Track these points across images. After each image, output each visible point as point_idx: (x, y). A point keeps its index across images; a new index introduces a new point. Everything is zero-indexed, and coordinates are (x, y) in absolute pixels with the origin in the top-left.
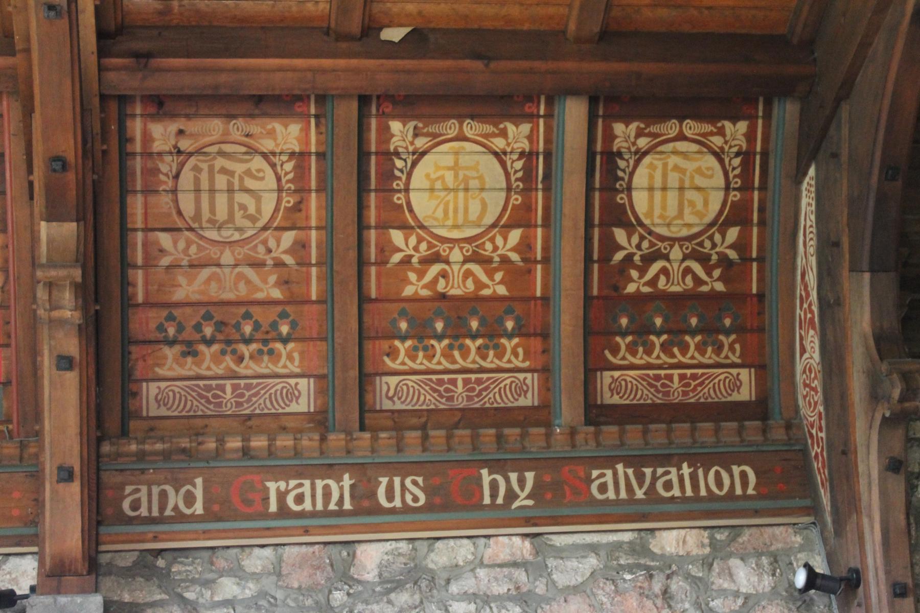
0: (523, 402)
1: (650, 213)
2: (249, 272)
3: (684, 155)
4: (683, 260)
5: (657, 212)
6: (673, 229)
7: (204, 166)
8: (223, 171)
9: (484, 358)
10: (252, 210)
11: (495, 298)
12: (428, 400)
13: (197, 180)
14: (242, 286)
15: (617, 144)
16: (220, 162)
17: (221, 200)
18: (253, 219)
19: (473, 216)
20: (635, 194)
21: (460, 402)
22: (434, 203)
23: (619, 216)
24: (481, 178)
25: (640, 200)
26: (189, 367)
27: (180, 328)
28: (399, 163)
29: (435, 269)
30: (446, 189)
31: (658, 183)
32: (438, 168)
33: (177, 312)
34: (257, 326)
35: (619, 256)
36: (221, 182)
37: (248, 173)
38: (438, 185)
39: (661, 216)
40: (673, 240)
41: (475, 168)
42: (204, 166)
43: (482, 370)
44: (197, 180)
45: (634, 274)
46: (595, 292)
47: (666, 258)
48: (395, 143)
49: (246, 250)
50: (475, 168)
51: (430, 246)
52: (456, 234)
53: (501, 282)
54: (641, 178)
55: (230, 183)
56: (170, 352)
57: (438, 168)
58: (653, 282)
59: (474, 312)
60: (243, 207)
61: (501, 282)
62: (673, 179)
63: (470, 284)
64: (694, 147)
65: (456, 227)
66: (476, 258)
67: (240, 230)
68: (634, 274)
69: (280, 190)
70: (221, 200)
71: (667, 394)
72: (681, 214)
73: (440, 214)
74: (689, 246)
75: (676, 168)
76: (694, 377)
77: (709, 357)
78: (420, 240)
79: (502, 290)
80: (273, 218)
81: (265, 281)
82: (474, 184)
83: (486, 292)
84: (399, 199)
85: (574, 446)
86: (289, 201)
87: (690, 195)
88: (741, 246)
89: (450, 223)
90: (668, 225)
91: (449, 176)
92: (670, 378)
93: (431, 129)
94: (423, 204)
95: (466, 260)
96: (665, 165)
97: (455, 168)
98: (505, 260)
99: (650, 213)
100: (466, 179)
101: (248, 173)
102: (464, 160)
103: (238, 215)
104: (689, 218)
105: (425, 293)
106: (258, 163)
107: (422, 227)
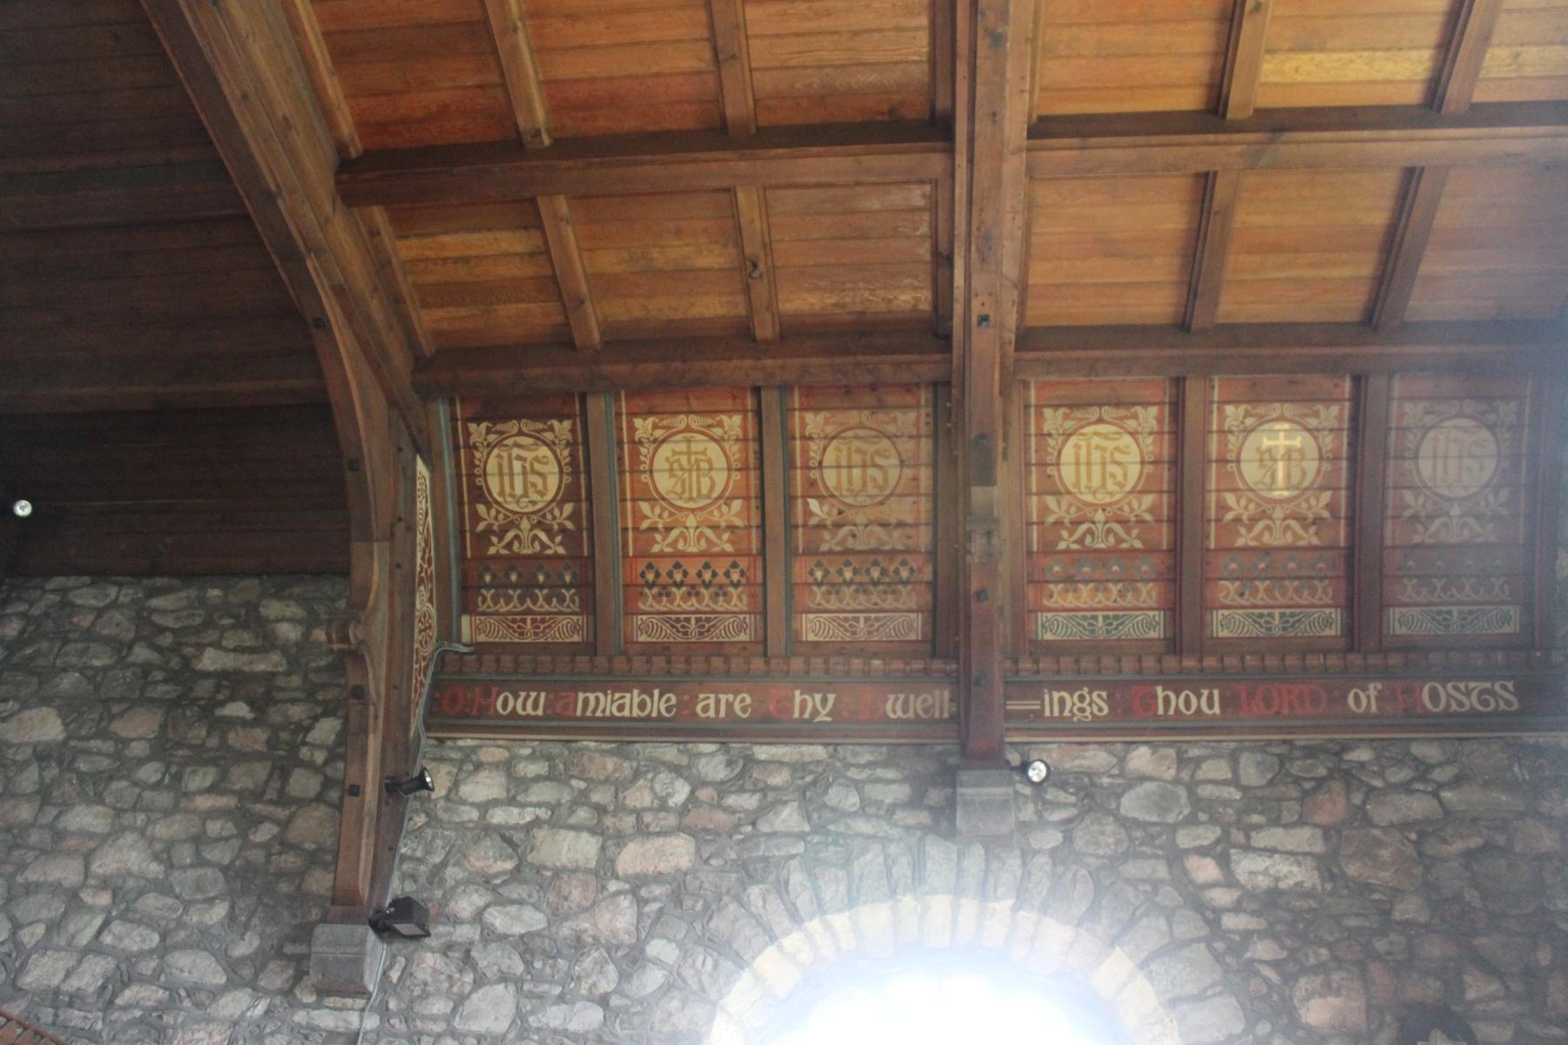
0: (912, 637)
1: (1077, 484)
2: (710, 533)
3: (1105, 437)
4: (1285, 519)
5: (1084, 482)
6: (1099, 496)
7: (505, 454)
8: (519, 458)
9: (716, 602)
10: (540, 486)
11: (556, 557)
12: (838, 635)
13: (500, 466)
14: (703, 542)
15: (1047, 427)
16: (516, 452)
17: (518, 481)
18: (542, 494)
19: (705, 491)
20: (489, 478)
21: (862, 636)
22: (673, 480)
23: (479, 494)
24: (709, 461)
25: (1068, 473)
26: (664, 605)
27: (658, 575)
28: (1051, 442)
29: (1083, 528)
30: (682, 469)
31: (844, 462)
32: (674, 453)
33: (682, 561)
34: (884, 572)
35: (481, 527)
36: (517, 466)
37: (536, 459)
38: (676, 466)
39: (1088, 487)
40: (1095, 507)
41: (704, 453)
42: (505, 454)
43: (714, 612)
44: (500, 466)
45: (494, 539)
46: (469, 554)
47: (518, 527)
48: (1047, 427)
49: (704, 514)
50: (704, 453)
51: (1079, 509)
52: (692, 505)
53: (561, 544)
54: (1068, 454)
55: (524, 467)
56: (489, 594)
57: (674, 453)
58: (1259, 537)
59: (540, 568)
60: (534, 485)
61: (561, 544)
62: (1096, 456)
63: (1111, 539)
64: (1114, 429)
65: (691, 499)
66: (540, 525)
67: (534, 503)
68: (494, 539)
69: (561, 471)
70: (518, 481)
71: (854, 633)
72: (526, 494)
73: (679, 489)
74: (535, 519)
75: (1098, 447)
76: (1116, 618)
77: (1129, 601)
78: (663, 509)
79: (561, 550)
80: (725, 489)
81: (720, 537)
82: (704, 465)
83: (1124, 546)
84: (479, 481)
85: (1120, 671)
86: (567, 479)
87: (1111, 468)
88: (575, 516)
89: (686, 495)
90: (1094, 493)
91: (684, 459)
92: (1271, 616)
93: (665, 423)
94: (664, 483)
95: (533, 527)
96: (510, 456)
97: (689, 453)
98: (1141, 521)
99: (1077, 484)
100: (697, 461)
101: (877, 452)
102: (696, 447)
103: (531, 490)
104: (872, 490)
105: (1075, 547)
106: (544, 451)
107: (663, 499)
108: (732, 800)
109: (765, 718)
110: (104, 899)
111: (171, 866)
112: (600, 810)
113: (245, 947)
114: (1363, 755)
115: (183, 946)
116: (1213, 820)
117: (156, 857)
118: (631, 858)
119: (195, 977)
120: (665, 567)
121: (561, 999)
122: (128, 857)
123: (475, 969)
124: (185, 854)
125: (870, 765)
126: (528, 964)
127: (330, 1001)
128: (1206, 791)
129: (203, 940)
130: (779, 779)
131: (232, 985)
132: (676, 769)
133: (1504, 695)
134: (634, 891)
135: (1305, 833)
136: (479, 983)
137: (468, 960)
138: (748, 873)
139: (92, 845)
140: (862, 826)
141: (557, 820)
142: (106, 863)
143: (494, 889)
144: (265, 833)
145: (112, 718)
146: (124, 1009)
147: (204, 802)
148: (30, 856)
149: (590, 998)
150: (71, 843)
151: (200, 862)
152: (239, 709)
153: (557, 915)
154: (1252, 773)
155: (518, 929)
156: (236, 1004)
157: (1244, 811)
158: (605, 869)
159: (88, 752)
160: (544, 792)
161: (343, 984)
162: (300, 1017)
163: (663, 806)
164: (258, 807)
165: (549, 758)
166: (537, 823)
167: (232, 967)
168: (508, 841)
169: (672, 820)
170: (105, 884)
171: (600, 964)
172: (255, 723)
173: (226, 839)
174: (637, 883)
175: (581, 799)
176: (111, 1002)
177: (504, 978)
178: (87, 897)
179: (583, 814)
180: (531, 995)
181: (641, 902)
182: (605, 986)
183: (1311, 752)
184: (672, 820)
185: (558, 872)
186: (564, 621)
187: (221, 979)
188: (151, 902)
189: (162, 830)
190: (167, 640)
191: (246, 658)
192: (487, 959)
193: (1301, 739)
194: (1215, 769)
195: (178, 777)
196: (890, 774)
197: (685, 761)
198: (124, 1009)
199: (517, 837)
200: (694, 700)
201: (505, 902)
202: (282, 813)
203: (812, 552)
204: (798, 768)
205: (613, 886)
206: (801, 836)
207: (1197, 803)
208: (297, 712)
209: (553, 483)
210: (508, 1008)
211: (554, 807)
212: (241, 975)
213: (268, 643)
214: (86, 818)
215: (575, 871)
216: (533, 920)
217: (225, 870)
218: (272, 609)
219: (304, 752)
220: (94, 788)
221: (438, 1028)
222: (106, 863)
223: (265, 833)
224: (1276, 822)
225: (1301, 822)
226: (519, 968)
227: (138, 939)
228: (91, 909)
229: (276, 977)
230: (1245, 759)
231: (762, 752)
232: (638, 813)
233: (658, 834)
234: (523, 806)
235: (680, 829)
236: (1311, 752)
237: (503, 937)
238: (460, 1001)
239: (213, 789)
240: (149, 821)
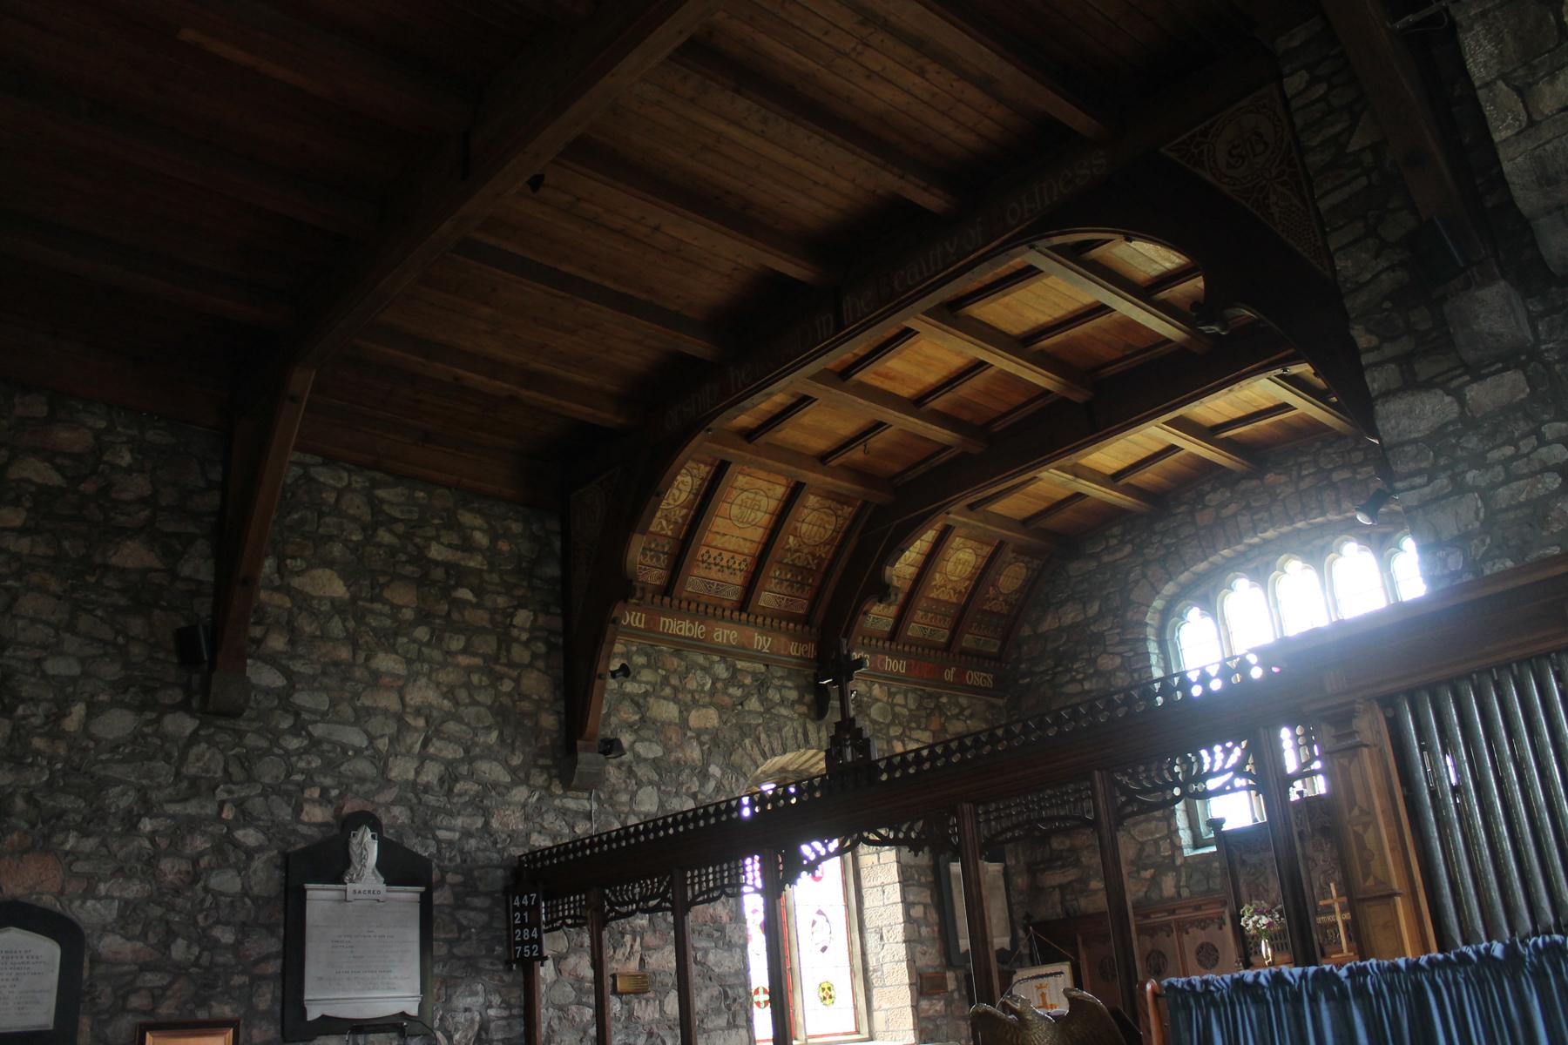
108: (731, 690)
109: (744, 647)
110: (421, 723)
111: (457, 703)
112: (675, 688)
113: (516, 761)
114: (944, 700)
115: (481, 757)
116: (900, 724)
117: (444, 696)
118: (695, 719)
119: (494, 777)
120: (714, 553)
121: (677, 794)
122: (422, 694)
123: (635, 776)
124: (463, 695)
125: (781, 678)
126: (660, 775)
127: (570, 793)
128: (898, 709)
129: (489, 754)
130: (748, 681)
131: (515, 783)
132: (703, 669)
133: (990, 683)
134: (698, 738)
135: (928, 734)
136: (640, 784)
137: (630, 771)
138: (744, 730)
139: (401, 683)
140: (784, 711)
141: (654, 692)
142: (415, 697)
143: (636, 732)
144: (507, 686)
145: (383, 586)
146: (460, 795)
147: (463, 660)
148: (360, 687)
149: (687, 794)
150: (386, 680)
151: (475, 703)
152: (465, 594)
153: (668, 750)
154: (912, 705)
155: (651, 756)
156: (520, 794)
157: (909, 722)
158: (684, 724)
159: (372, 612)
160: (647, 675)
161: (591, 784)
162: (557, 802)
163: (702, 691)
164: (498, 668)
165: (648, 655)
166: (646, 694)
167: (513, 771)
168: (637, 704)
169: (707, 699)
170: (418, 712)
171: (690, 777)
172: (478, 606)
173: (485, 687)
174: (699, 734)
175: (665, 681)
176: (450, 790)
177: (651, 783)
178: (410, 719)
179: (668, 691)
180: (664, 792)
181: (701, 744)
182: (695, 788)
183: (930, 696)
184: (707, 699)
185: (663, 724)
186: (656, 572)
187: (508, 779)
188: (452, 727)
189: (442, 677)
190: (400, 528)
191: (459, 554)
192: (643, 772)
193: (928, 689)
194: (899, 699)
195: (440, 639)
196: (789, 684)
197: (706, 664)
198: (460, 795)
199: (641, 701)
200: (713, 631)
201: (642, 740)
202: (515, 674)
203: (780, 562)
204: (754, 674)
205: (689, 734)
206: (761, 714)
207: (895, 715)
208: (501, 601)
209: (684, 496)
210: (656, 799)
211: (654, 685)
212: (520, 777)
213: (467, 546)
214: (387, 663)
215: (670, 724)
216: (656, 751)
217: (490, 708)
218: (467, 518)
219: (515, 632)
220: (387, 639)
221: (626, 809)
222: (415, 697)
223: (507, 686)
224: (918, 727)
225: (926, 729)
226: (656, 778)
227: (452, 752)
228: (416, 729)
229: (539, 779)
230: (910, 696)
231: (740, 665)
232: (692, 692)
233: (704, 706)
234: (640, 682)
235: (711, 704)
236: (930, 696)
237: (646, 760)
238: (633, 796)
239: (465, 651)
240: (431, 670)
